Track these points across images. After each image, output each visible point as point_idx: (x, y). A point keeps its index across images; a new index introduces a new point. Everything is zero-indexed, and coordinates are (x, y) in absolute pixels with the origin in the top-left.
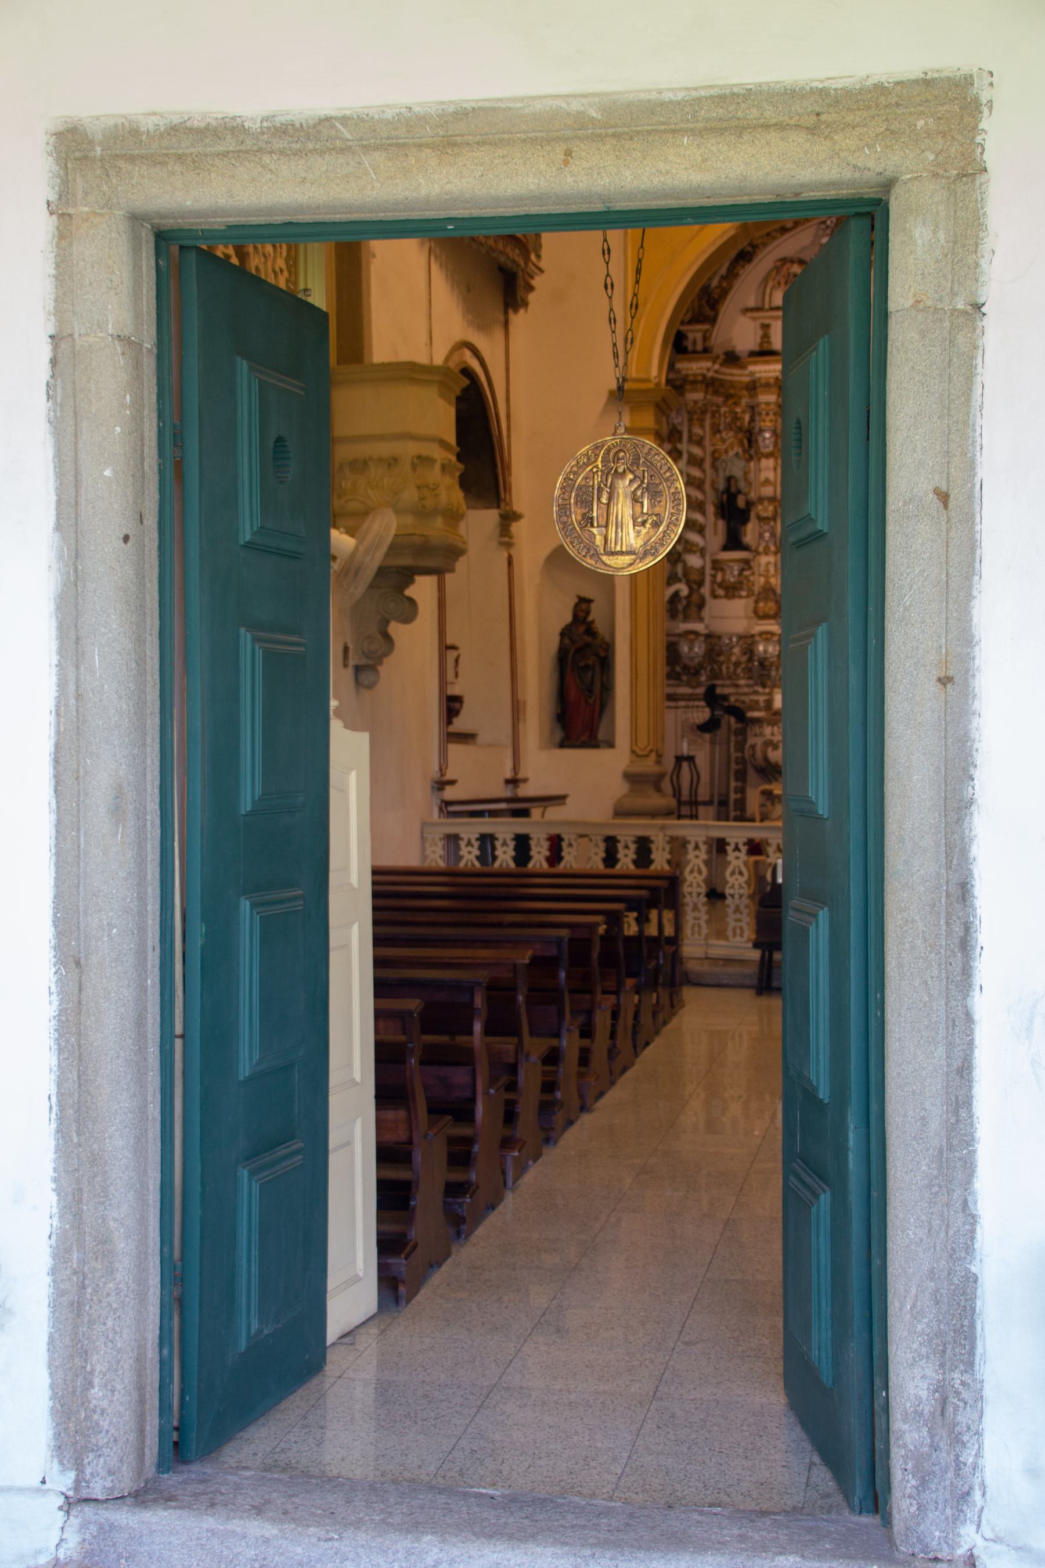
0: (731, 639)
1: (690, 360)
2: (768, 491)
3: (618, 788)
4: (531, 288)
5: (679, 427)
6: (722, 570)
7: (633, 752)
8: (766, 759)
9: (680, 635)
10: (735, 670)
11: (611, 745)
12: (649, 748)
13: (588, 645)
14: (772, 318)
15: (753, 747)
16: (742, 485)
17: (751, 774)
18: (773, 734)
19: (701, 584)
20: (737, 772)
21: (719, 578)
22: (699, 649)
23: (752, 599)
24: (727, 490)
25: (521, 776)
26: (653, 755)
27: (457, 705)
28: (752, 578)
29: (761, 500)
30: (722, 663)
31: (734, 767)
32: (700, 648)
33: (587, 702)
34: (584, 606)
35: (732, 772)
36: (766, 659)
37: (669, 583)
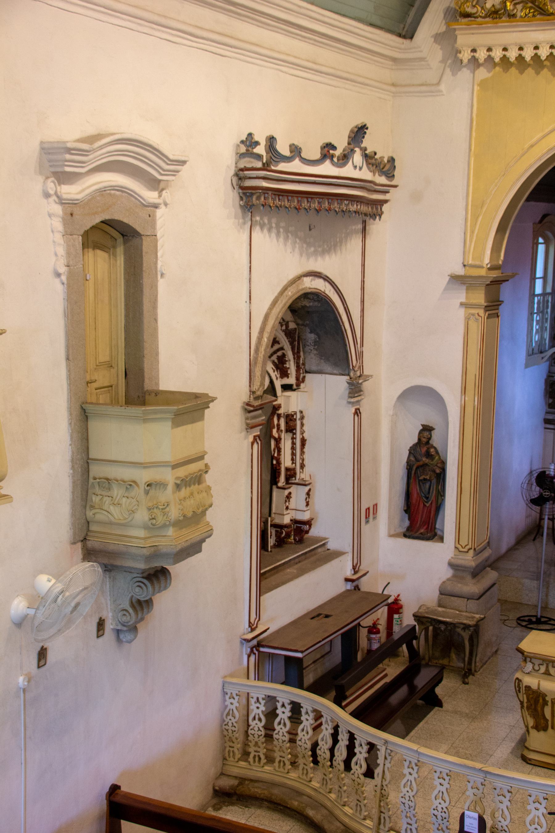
7: (456, 547)
11: (441, 539)
12: (468, 547)
13: (426, 465)
26: (472, 552)
27: (306, 527)
33: (425, 505)
34: (426, 434)
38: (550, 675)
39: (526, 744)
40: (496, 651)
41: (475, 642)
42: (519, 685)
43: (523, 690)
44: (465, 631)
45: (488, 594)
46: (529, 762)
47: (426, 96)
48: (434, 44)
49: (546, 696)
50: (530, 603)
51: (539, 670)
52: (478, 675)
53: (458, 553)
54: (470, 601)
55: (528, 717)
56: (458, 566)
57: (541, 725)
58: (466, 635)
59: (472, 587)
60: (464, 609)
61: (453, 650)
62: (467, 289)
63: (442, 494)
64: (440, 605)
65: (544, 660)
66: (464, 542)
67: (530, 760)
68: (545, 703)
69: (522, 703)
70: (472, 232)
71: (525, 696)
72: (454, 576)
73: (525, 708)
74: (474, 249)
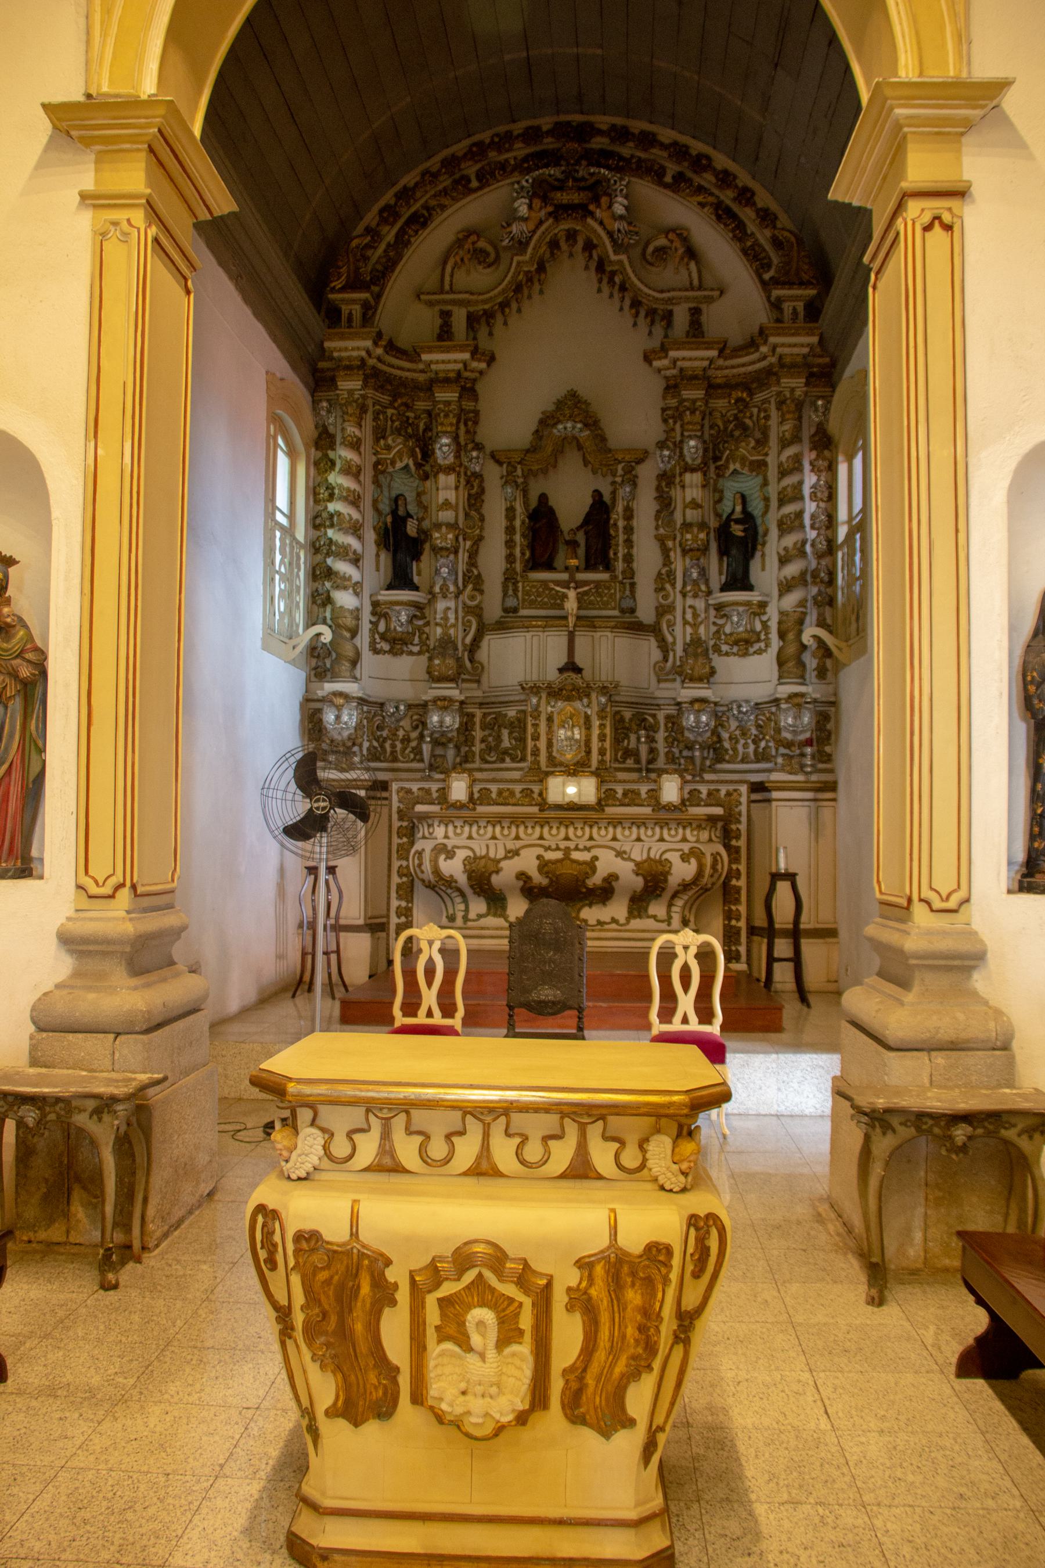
0: (397, 708)
1: (342, 337)
2: (446, 516)
5: (331, 429)
6: (386, 616)
7: (79, 887)
8: (437, 871)
9: (322, 700)
10: (404, 749)
14: (454, 302)
15: (420, 853)
16: (412, 508)
17: (419, 890)
18: (446, 837)
19: (354, 632)
20: (399, 887)
21: (382, 627)
22: (350, 717)
23: (424, 658)
24: (394, 512)
26: (125, 894)
28: (427, 630)
29: (438, 526)
30: (385, 740)
32: (350, 715)
35: (394, 888)
36: (443, 734)
38: (398, 1169)
39: (309, 1489)
40: (211, 1194)
41: (140, 1159)
44: (100, 1120)
49: (388, 1262)
51: (351, 1156)
52: (151, 1260)
53: (85, 903)
54: (122, 1038)
55: (314, 1371)
56: (85, 940)
57: (370, 1394)
58: (104, 1134)
59: (126, 997)
60: (107, 1063)
61: (77, 1194)
62: (97, 162)
63: (41, 745)
64: (34, 1062)
65: (370, 1107)
66: (100, 867)
68: (384, 1294)
69: (283, 1314)
71: (296, 1280)
72: (77, 974)
73: (299, 1333)
74: (114, 57)
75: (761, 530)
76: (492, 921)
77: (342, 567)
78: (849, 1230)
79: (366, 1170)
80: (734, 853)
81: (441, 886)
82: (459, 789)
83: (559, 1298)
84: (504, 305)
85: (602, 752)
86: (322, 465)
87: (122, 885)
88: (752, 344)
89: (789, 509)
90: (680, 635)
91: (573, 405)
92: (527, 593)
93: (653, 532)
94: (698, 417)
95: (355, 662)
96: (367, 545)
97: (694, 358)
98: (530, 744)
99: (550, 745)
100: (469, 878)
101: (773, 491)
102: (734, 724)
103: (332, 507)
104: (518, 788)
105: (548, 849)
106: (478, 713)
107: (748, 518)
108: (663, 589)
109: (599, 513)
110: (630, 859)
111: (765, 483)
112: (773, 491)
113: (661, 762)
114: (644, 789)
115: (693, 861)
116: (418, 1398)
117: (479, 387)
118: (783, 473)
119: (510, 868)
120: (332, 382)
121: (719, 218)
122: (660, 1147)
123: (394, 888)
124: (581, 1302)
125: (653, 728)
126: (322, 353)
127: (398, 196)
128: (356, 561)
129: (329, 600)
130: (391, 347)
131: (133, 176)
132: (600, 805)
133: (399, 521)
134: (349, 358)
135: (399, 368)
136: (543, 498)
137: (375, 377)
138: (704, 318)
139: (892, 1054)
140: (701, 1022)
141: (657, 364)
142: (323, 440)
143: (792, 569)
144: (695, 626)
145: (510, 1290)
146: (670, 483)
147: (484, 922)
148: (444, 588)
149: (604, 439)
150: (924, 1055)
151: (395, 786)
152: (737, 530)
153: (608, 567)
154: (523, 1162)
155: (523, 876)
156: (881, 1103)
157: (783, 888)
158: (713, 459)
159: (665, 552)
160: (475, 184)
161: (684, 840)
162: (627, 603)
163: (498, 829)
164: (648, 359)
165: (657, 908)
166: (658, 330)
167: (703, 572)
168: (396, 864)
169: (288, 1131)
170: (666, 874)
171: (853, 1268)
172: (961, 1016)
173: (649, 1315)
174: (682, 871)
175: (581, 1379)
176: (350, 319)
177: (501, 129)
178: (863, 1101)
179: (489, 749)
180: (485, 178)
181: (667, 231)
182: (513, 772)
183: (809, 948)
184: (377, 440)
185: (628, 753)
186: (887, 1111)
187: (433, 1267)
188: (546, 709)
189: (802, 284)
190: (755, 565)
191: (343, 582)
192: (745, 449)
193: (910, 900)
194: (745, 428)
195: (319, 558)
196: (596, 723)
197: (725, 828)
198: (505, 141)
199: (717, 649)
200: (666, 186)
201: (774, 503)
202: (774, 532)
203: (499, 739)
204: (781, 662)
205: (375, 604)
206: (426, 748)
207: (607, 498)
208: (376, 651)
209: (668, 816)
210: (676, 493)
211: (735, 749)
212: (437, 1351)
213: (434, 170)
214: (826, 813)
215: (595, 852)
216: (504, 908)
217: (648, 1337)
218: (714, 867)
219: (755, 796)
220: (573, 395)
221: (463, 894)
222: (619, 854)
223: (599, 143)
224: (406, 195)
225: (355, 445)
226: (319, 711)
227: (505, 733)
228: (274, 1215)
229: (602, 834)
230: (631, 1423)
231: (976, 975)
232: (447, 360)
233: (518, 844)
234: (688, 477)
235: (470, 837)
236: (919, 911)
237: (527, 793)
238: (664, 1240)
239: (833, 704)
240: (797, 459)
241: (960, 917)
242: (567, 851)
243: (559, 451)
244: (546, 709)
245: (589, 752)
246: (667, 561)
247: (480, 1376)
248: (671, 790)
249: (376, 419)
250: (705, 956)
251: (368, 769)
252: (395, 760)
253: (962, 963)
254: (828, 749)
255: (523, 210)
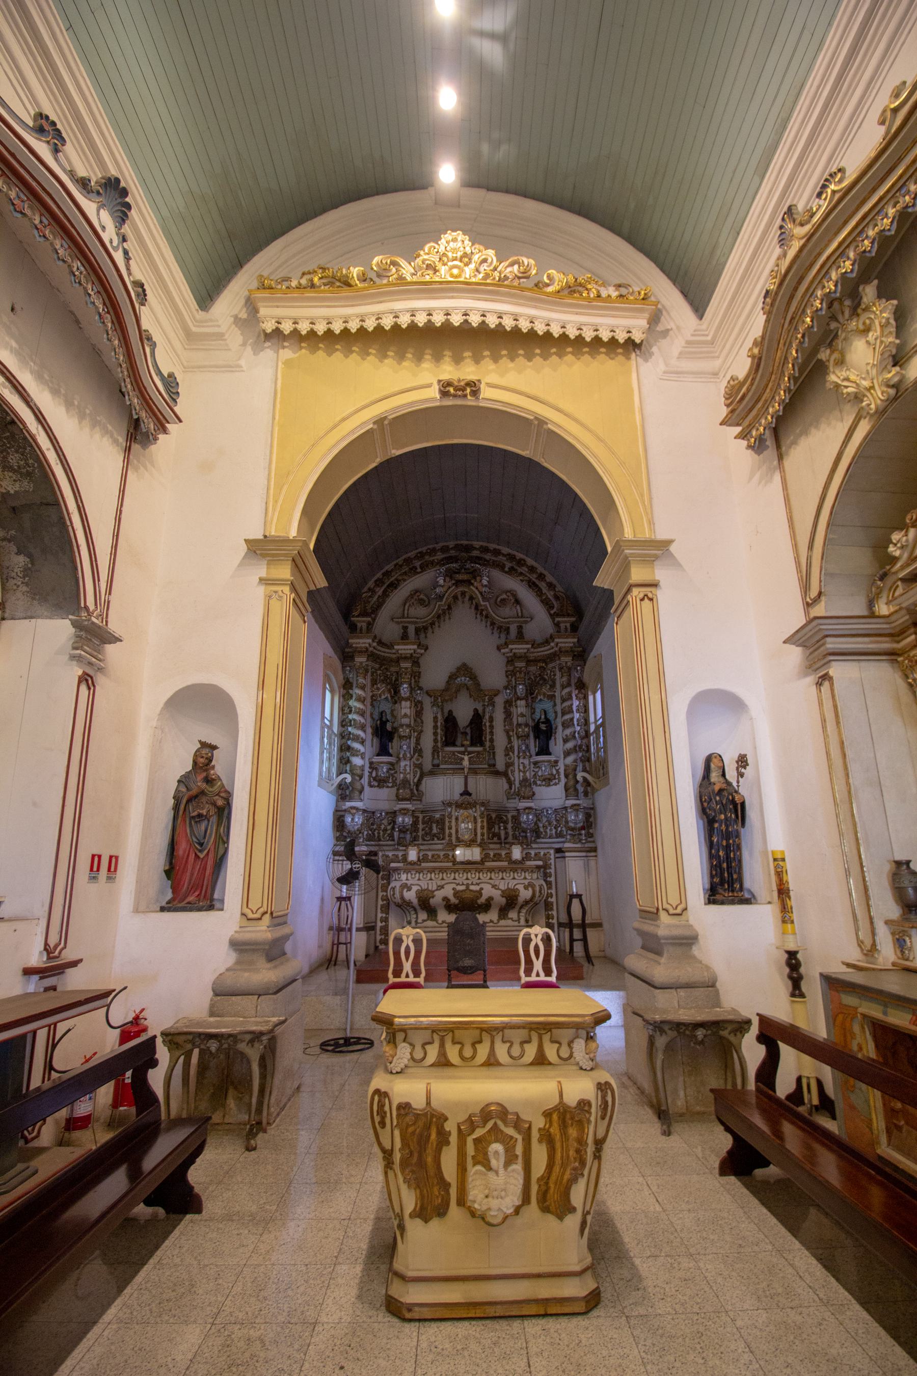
1: (358, 638)
2: (405, 721)
3: (221, 959)
4: (165, 431)
5: (351, 680)
7: (243, 914)
8: (402, 898)
9: (345, 811)
10: (384, 835)
12: (262, 910)
14: (409, 622)
15: (394, 888)
16: (389, 717)
18: (407, 879)
19: (361, 777)
20: (382, 906)
21: (374, 774)
22: (359, 819)
24: (381, 719)
25: (69, 955)
26: (267, 916)
29: (402, 726)
31: (380, 903)
35: (379, 907)
36: (404, 827)
37: (339, 773)
39: (398, 1266)
42: (381, 1106)
43: (392, 1116)
45: (290, 988)
46: (408, 1316)
47: (223, 372)
48: (234, 326)
49: (446, 1119)
50: (332, 1027)
51: (424, 1058)
55: (404, 1188)
62: (268, 564)
63: (225, 839)
67: (410, 1307)
68: (443, 1138)
69: (388, 1155)
70: (276, 502)
71: (397, 1133)
73: (397, 1166)
75: (554, 727)
76: (430, 923)
77: (356, 745)
78: (642, 1092)
79: (432, 1065)
80: (549, 884)
81: (404, 906)
82: (413, 855)
83: (535, 1135)
84: (433, 624)
85: (482, 835)
86: (346, 696)
87: (266, 913)
88: (547, 642)
89: (567, 717)
90: (517, 777)
91: (464, 669)
92: (444, 757)
93: (503, 728)
94: (522, 675)
95: (361, 792)
96: (367, 735)
97: (520, 648)
98: (447, 831)
99: (457, 831)
100: (419, 901)
101: (559, 709)
102: (545, 819)
103: (350, 717)
104: (442, 854)
105: (458, 884)
106: (421, 816)
107: (547, 721)
108: (508, 755)
109: (477, 719)
110: (498, 889)
111: (555, 705)
112: (559, 709)
113: (510, 839)
114: (503, 853)
115: (530, 889)
116: (461, 1202)
117: (421, 661)
118: (563, 700)
119: (439, 895)
120: (352, 658)
121: (530, 586)
122: (579, 1045)
123: (379, 907)
124: (547, 1137)
125: (506, 822)
126: (348, 644)
127: (384, 574)
128: (363, 742)
129: (348, 761)
130: (380, 643)
131: (285, 572)
132: (482, 862)
133: (384, 723)
134: (361, 647)
135: (384, 652)
136: (450, 712)
137: (373, 656)
138: (524, 631)
139: (658, 991)
140: (546, 976)
141: (503, 651)
142: (347, 685)
143: (570, 745)
144: (524, 772)
145: (510, 1131)
146: (511, 705)
147: (426, 924)
148: (405, 755)
149: (479, 685)
150: (673, 991)
151: (380, 854)
152: (543, 727)
153: (482, 745)
154: (511, 1057)
155: (446, 899)
156: (658, 1017)
157: (575, 902)
158: (530, 694)
159: (509, 737)
160: (419, 570)
161: (525, 878)
162: (492, 762)
163: (433, 875)
164: (499, 648)
165: (513, 914)
166: (503, 636)
167: (527, 747)
168: (381, 894)
169: (391, 1045)
170: (517, 896)
171: (648, 1114)
172: (690, 969)
173: (581, 1142)
174: (525, 894)
175: (547, 1183)
176: (361, 630)
177: (431, 547)
178: (649, 1016)
179: (426, 834)
180: (423, 568)
181: (506, 592)
182: (438, 846)
183: (590, 933)
184: (373, 685)
185: (494, 835)
186: (662, 1022)
187: (470, 1121)
188: (455, 814)
189: (568, 615)
190: (552, 743)
191: (356, 753)
192: (545, 689)
193: (658, 909)
194: (545, 680)
195: (344, 740)
196: (479, 820)
197: (544, 870)
198: (433, 551)
199: (535, 783)
200: (506, 572)
201: (559, 714)
202: (560, 728)
203: (431, 829)
204: (566, 789)
205: (371, 763)
206: (396, 834)
207: (480, 712)
208: (371, 786)
209: (515, 866)
210: (513, 710)
211: (546, 832)
212: (474, 1170)
213: (400, 563)
214: (592, 863)
215: (482, 885)
216: (436, 916)
217: (581, 1156)
218: (540, 892)
219: (557, 855)
220: (464, 665)
221: (415, 910)
222: (494, 886)
223: (475, 553)
224: (387, 574)
225: (363, 688)
226: (343, 816)
227: (434, 826)
228: (386, 1094)
229: (485, 876)
230: (574, 1210)
231: (694, 948)
232: (406, 649)
233: (443, 882)
234: (518, 702)
235: (419, 879)
236: (663, 914)
237: (446, 856)
238: (586, 1097)
239: (592, 809)
240: (570, 694)
241: (683, 917)
242: (468, 885)
243: (458, 691)
244: (455, 814)
245: (476, 835)
246: (510, 742)
247: (497, 1186)
248: (517, 853)
249: (372, 675)
250: (547, 939)
251: (367, 845)
252: (380, 840)
253: (687, 941)
254: (591, 831)
255: (441, 582)
